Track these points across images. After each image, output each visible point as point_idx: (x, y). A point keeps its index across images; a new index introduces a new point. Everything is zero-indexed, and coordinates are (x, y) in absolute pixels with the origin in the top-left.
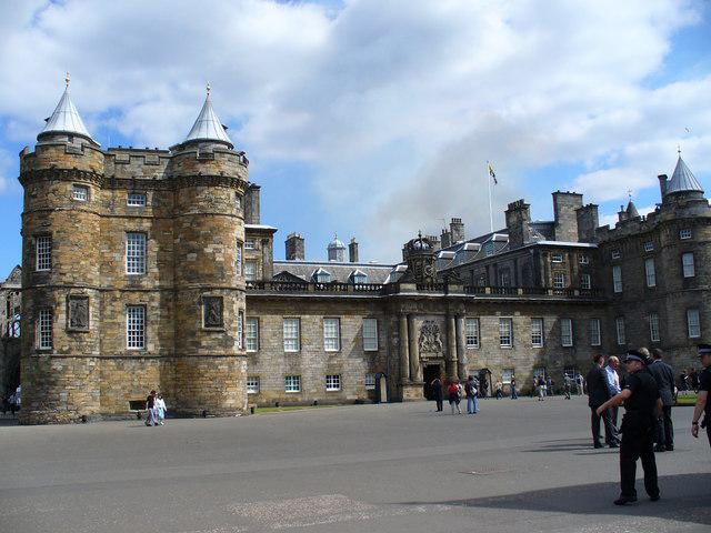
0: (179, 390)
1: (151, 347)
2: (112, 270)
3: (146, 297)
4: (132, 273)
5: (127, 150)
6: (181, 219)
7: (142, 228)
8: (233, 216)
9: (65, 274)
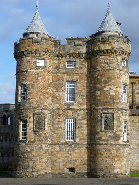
0: (91, 163)
1: (77, 140)
2: (59, 100)
3: (75, 115)
4: (69, 102)
6: (93, 73)
8: (119, 70)
9: (32, 103)
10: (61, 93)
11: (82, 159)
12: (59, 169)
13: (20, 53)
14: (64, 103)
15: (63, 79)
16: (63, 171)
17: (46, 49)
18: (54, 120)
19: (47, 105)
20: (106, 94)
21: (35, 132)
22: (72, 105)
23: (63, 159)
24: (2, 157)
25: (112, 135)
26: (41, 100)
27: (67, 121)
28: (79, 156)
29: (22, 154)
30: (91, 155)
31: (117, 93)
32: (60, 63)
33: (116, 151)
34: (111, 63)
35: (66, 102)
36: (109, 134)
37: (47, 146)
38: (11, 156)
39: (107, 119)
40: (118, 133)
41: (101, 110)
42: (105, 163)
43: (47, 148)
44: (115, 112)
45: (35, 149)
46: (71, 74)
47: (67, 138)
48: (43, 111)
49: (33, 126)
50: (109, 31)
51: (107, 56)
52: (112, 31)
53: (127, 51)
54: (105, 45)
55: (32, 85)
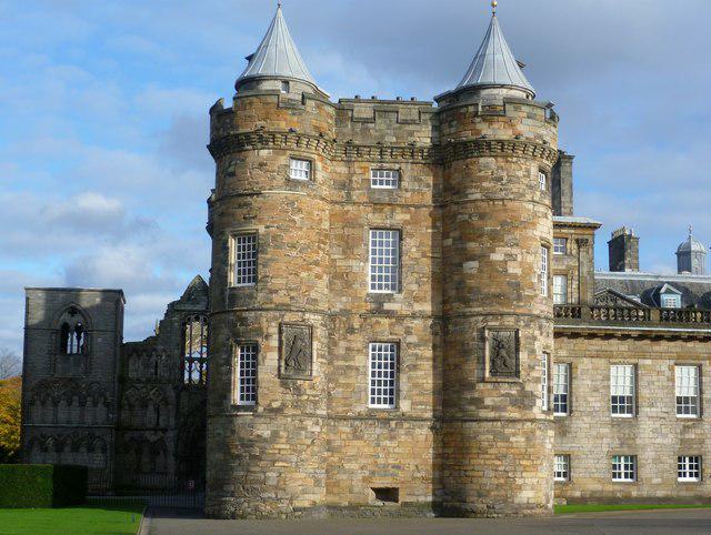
0: (447, 473)
1: (405, 406)
2: (348, 285)
3: (399, 329)
4: (377, 291)
5: (367, 102)
6: (455, 208)
7: (394, 222)
10: (355, 265)
11: (418, 461)
12: (351, 492)
13: (236, 136)
14: (364, 293)
15: (361, 221)
16: (362, 496)
17: (316, 128)
18: (335, 344)
19: (316, 300)
20: (498, 271)
21: (284, 380)
22: (389, 301)
23: (363, 461)
24: (55, 454)
25: (513, 392)
26: (301, 282)
27: (374, 350)
28: (409, 455)
29: (243, 445)
30: (446, 451)
31: (528, 270)
32: (351, 174)
33: (523, 439)
34: (510, 181)
35: (371, 291)
36: (504, 389)
37: (317, 424)
38: (83, 449)
39: (498, 346)
40: (528, 388)
41: (481, 318)
42: (492, 474)
43: (317, 429)
44: (522, 323)
45: (285, 430)
46: (387, 209)
47: (373, 402)
48: (307, 316)
49: (279, 363)
50: (502, 86)
51: (500, 159)
52: (510, 87)
53: (552, 146)
54: (496, 126)
55: (275, 238)
